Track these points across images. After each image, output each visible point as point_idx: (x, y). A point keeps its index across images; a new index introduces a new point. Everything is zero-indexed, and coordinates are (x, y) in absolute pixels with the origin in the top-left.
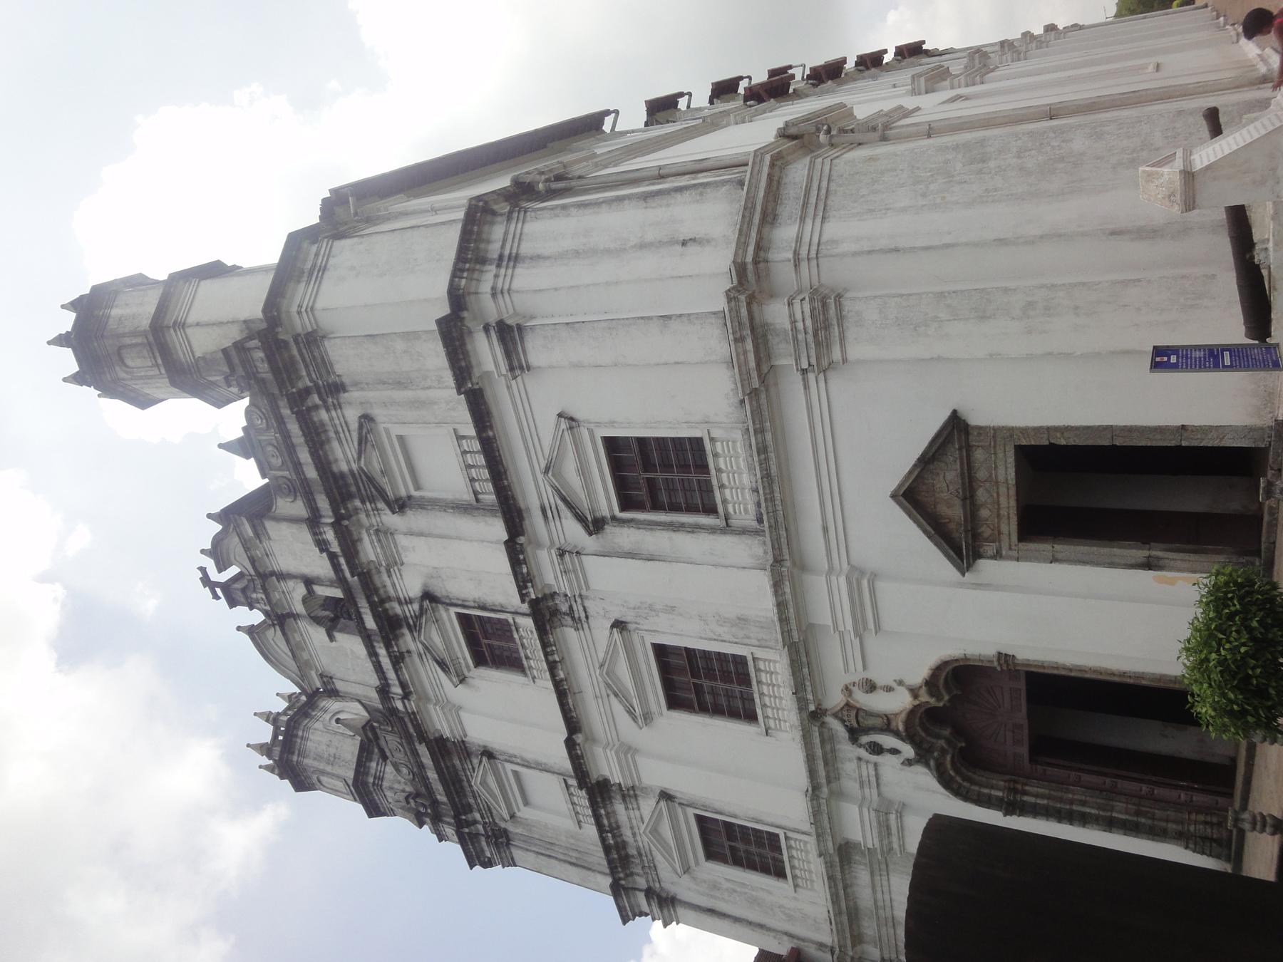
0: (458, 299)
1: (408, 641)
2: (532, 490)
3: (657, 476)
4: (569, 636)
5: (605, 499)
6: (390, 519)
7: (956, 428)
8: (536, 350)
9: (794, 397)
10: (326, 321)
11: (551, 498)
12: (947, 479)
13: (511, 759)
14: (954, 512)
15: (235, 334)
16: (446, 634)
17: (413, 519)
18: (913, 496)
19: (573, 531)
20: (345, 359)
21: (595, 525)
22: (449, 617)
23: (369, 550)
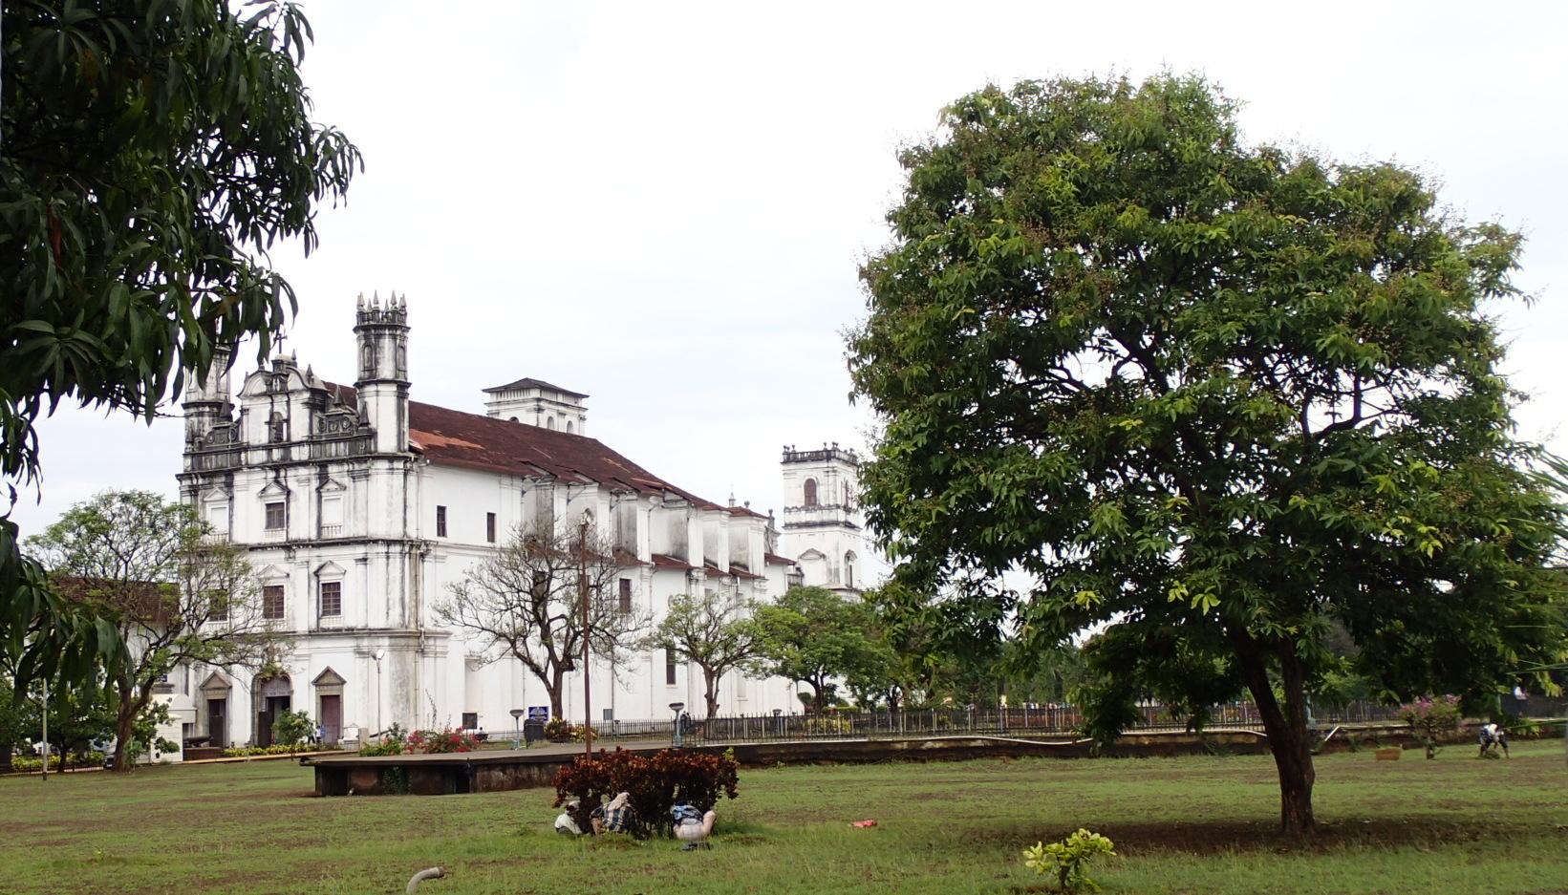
0: (375, 542)
1: (272, 474)
2: (327, 553)
3: (330, 596)
4: (282, 554)
5: (324, 579)
6: (315, 484)
7: (343, 682)
8: (361, 567)
9: (349, 643)
10: (373, 478)
11: (324, 560)
12: (334, 680)
13: (231, 509)
14: (325, 680)
15: (373, 425)
16: (275, 495)
17: (314, 495)
18: (328, 671)
19: (314, 567)
20: (361, 484)
21: (317, 574)
22: (282, 499)
23: (303, 472)
